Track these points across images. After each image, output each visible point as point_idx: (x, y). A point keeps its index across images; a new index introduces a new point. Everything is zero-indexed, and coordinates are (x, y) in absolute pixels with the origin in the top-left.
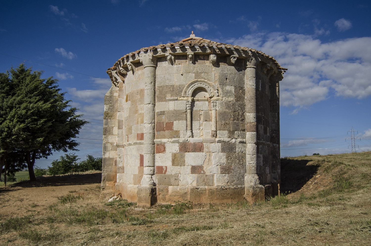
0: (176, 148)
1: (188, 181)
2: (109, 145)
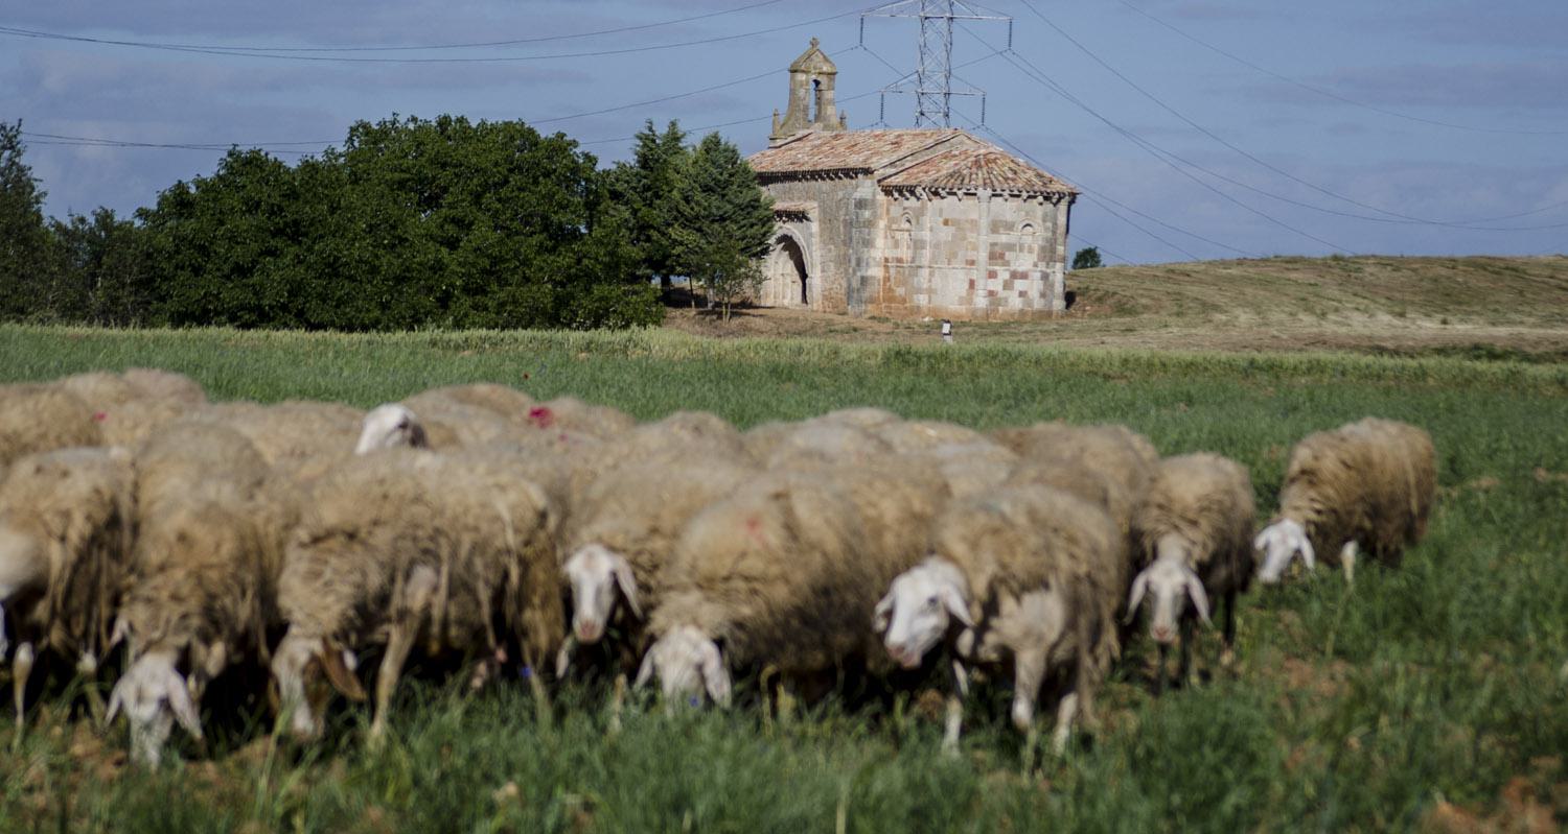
0: (1007, 276)
1: (1015, 303)
2: (870, 260)
